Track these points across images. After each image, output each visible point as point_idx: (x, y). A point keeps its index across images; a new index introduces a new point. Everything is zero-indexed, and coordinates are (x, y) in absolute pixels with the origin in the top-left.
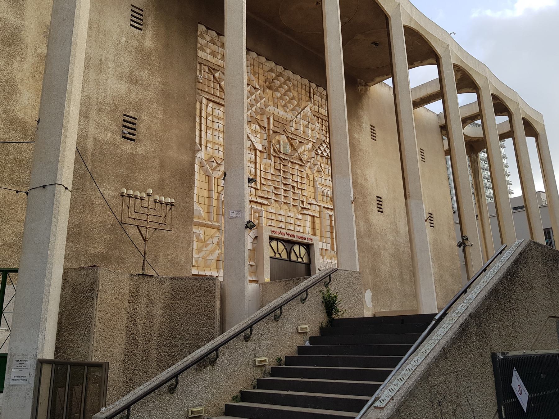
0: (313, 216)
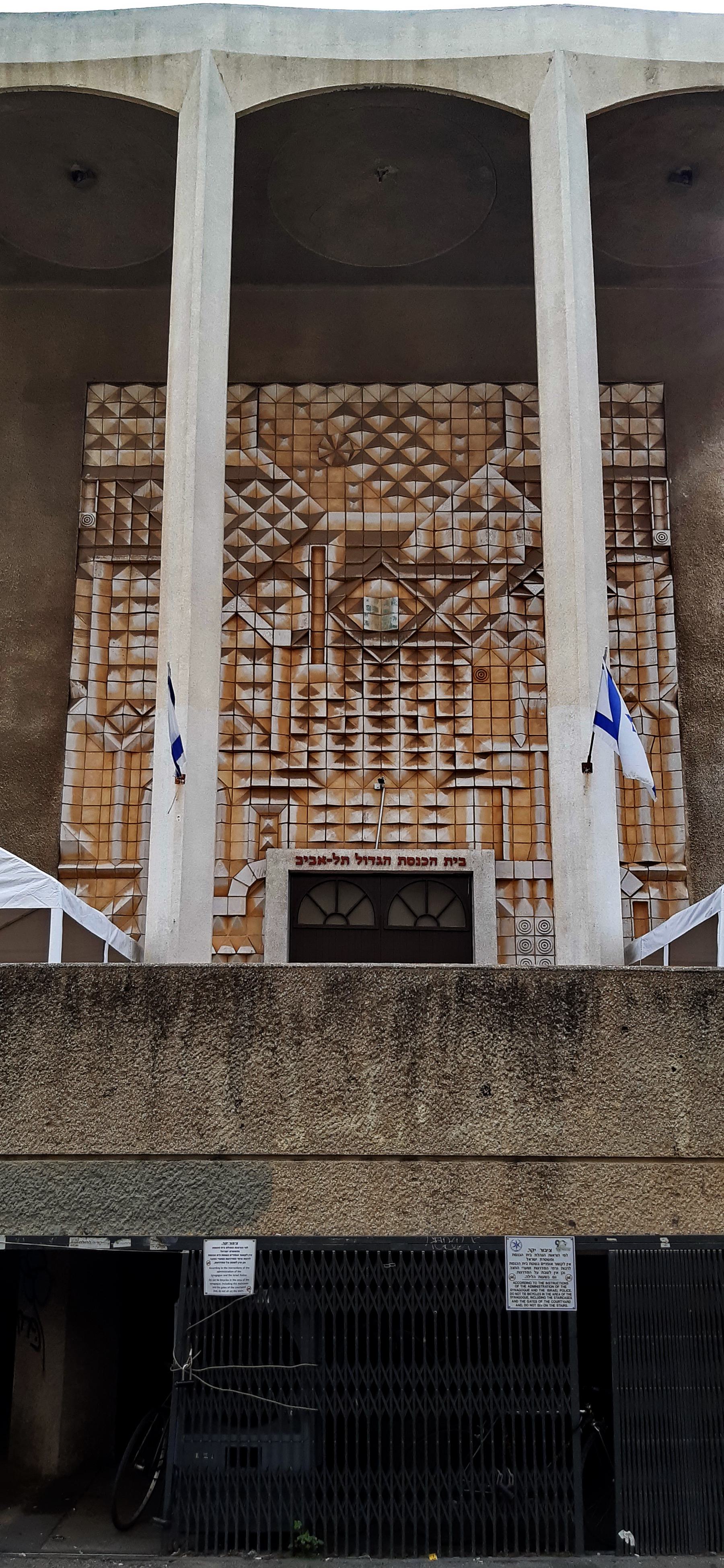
0: (493, 789)
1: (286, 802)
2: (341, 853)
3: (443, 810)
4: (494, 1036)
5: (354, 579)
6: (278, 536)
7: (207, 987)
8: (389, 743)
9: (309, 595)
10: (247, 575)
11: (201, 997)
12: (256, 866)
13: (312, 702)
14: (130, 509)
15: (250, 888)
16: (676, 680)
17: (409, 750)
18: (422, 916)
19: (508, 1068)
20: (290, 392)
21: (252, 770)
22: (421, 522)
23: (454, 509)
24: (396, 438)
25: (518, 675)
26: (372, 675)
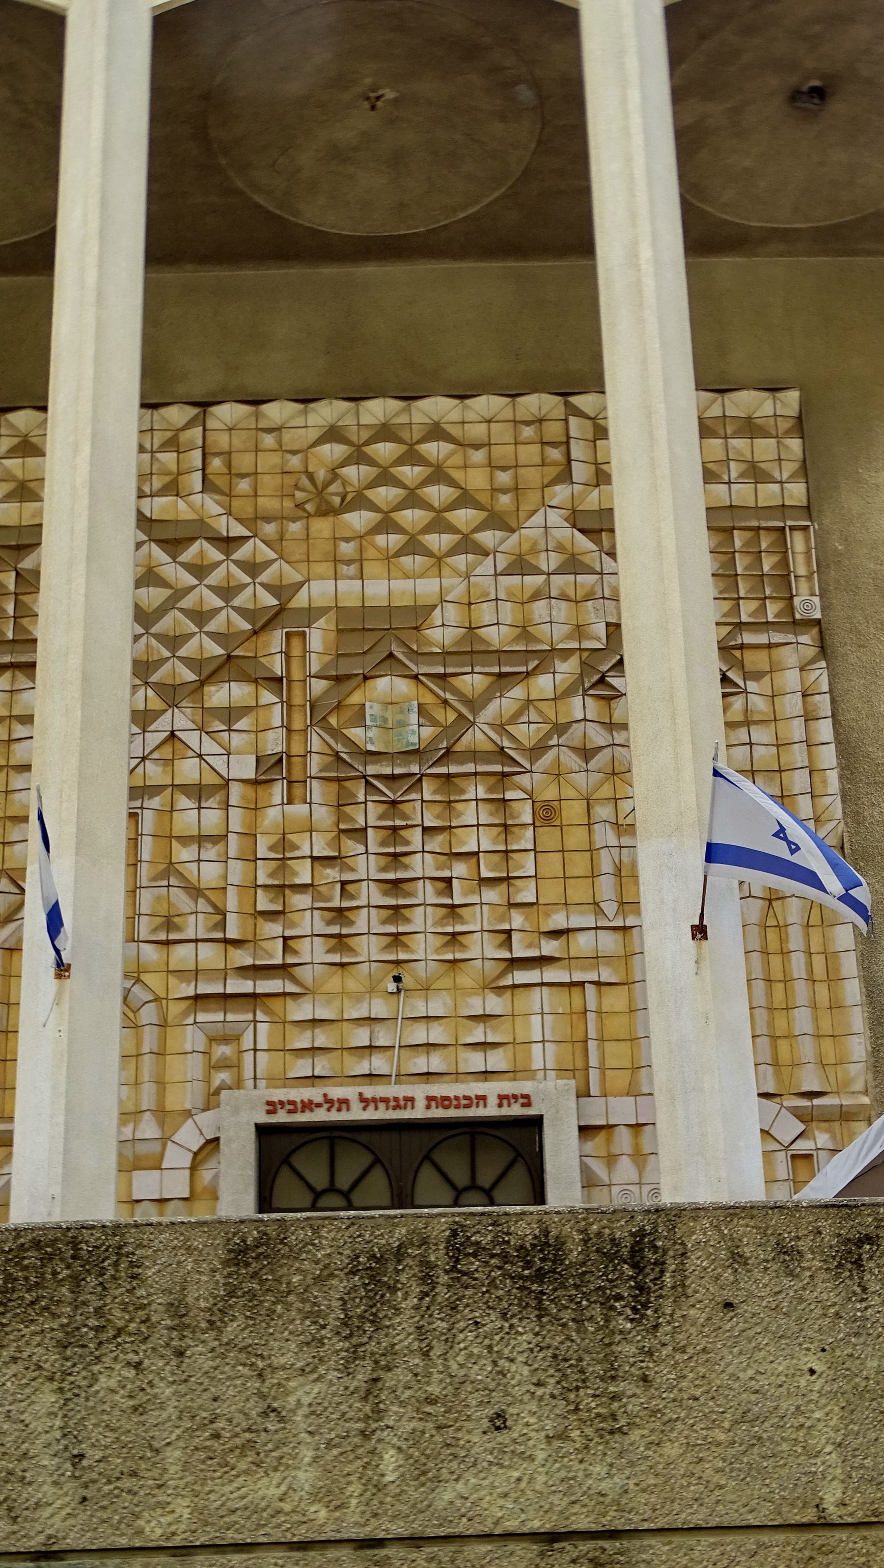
1: (250, 1017)
2: (337, 1092)
3: (495, 1022)
4: (511, 1326)
5: (349, 677)
6: (235, 617)
7: (26, 1262)
8: (408, 920)
9: (282, 702)
10: (189, 676)
11: (16, 1279)
12: (204, 1118)
13: (289, 862)
14: (12, 588)
15: (196, 1154)
16: (839, 814)
17: (440, 930)
18: (467, 1189)
19: (535, 1380)
20: (250, 415)
21: (197, 971)
22: (448, 593)
23: (498, 571)
24: (409, 473)
25: (603, 812)
26: (381, 817)
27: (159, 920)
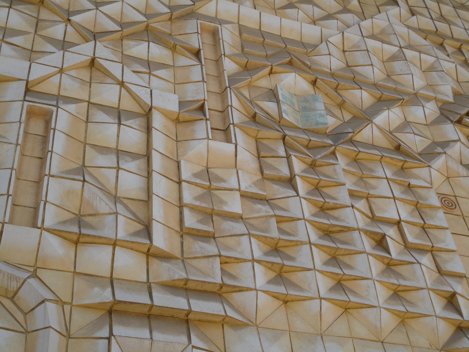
27: (68, 216)
